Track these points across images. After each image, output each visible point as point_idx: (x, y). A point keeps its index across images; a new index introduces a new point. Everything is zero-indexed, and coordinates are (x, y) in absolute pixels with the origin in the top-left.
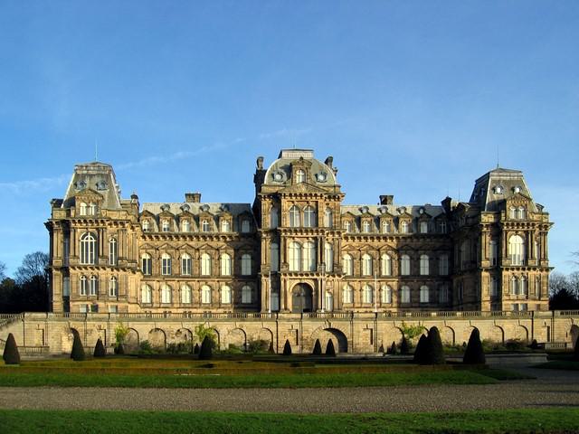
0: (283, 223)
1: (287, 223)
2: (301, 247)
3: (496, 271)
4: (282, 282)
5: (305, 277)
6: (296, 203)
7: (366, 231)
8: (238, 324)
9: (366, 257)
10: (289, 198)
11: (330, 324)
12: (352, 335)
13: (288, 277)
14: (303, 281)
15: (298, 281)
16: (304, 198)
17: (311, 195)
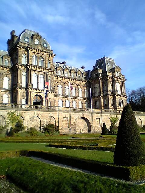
0: (30, 63)
1: (33, 62)
2: (38, 77)
3: (114, 95)
4: (29, 93)
5: (40, 91)
6: (36, 54)
7: (59, 74)
8: (36, 112)
9: (60, 86)
10: (33, 50)
11: (83, 115)
12: (93, 122)
13: (33, 90)
14: (39, 94)
15: (36, 94)
16: (40, 52)
17: (43, 51)
